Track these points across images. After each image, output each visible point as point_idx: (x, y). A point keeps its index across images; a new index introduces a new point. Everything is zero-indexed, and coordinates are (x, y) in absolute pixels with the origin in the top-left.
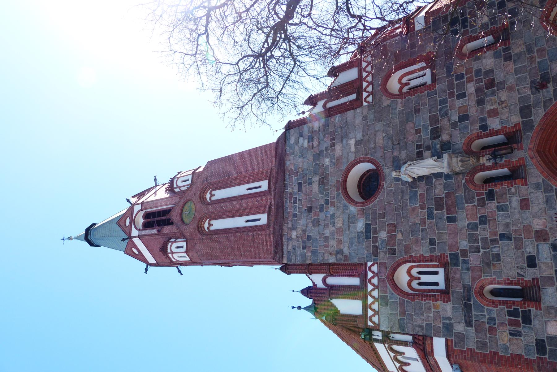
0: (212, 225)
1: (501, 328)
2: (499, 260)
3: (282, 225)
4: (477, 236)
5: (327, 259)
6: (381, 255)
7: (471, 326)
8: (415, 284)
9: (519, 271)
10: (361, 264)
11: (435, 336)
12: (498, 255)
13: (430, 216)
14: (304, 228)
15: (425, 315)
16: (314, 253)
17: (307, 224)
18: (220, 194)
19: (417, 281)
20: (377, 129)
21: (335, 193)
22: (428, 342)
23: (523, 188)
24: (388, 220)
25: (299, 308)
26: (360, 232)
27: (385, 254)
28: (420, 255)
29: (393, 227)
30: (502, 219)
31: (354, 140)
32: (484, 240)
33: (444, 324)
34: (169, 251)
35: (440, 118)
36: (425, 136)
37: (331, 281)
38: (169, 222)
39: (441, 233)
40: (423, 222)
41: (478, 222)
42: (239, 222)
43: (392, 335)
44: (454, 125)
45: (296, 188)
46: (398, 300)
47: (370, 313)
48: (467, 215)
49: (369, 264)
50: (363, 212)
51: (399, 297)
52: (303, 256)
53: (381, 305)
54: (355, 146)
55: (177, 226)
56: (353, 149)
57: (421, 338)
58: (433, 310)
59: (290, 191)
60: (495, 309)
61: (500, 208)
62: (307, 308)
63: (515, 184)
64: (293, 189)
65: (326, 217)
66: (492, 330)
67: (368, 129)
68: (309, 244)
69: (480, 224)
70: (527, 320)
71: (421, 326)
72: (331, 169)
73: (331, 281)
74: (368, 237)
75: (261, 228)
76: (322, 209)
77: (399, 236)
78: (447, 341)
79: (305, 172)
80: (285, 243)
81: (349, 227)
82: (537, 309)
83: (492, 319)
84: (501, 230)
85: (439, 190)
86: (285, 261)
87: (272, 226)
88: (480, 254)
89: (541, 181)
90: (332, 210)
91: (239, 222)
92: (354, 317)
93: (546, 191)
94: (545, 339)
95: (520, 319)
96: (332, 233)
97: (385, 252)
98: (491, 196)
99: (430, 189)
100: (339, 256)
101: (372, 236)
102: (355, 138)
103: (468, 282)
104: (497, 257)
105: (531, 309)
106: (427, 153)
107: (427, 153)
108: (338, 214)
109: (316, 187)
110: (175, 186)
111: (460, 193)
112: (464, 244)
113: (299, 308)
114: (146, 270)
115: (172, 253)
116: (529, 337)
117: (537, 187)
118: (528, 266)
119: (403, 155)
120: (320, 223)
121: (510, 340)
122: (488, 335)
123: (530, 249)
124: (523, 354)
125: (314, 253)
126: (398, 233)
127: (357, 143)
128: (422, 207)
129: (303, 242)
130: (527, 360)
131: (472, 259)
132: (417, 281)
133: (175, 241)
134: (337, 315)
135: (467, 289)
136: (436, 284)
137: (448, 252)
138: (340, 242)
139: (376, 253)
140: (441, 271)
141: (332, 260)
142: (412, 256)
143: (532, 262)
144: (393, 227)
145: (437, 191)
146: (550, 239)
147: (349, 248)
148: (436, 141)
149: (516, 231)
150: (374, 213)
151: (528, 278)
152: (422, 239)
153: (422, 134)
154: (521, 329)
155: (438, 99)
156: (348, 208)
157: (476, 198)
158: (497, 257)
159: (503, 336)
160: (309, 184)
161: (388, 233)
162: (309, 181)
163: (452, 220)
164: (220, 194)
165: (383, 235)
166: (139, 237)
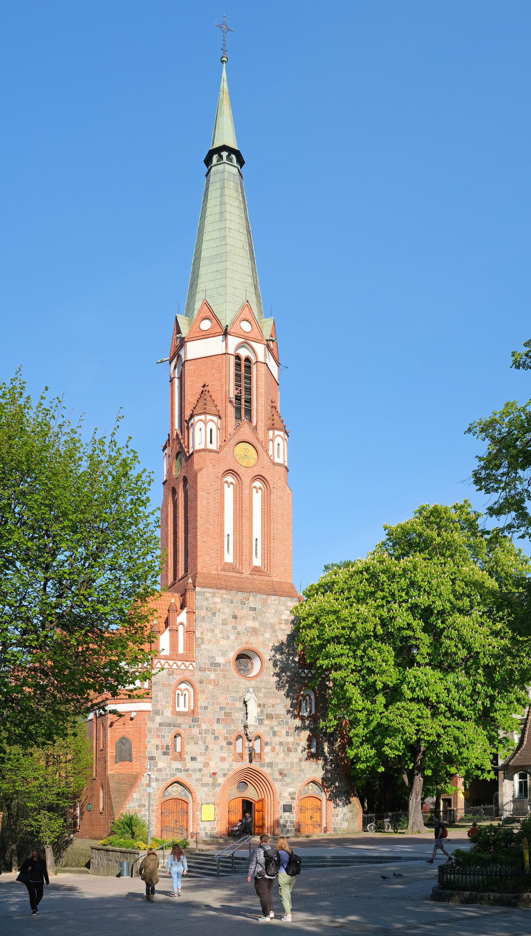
2: (195, 744)
3: (226, 589)
6: (200, 673)
13: (222, 708)
14: (221, 610)
16: (203, 619)
17: (224, 614)
19: (180, 694)
21: (244, 641)
23: (230, 759)
24: (221, 680)
29: (216, 684)
30: (216, 747)
32: (206, 738)
36: (270, 710)
40: (218, 704)
44: (272, 728)
49: (194, 664)
52: (201, 608)
55: (234, 435)
61: (222, 747)
68: (209, 614)
72: (261, 639)
74: (211, 664)
76: (234, 628)
77: (211, 687)
79: (263, 614)
90: (232, 637)
93: (228, 769)
98: (229, 743)
99: (238, 710)
100: (200, 640)
106: (259, 710)
111: (233, 727)
112: (204, 727)
117: (231, 766)
123: (199, 759)
125: (203, 619)
128: (227, 704)
129: (211, 609)
132: (180, 694)
135: (179, 726)
138: (210, 641)
139: (201, 670)
140: (186, 710)
141: (198, 634)
143: (193, 759)
144: (216, 684)
145: (236, 714)
148: (265, 717)
150: (227, 671)
151: (185, 756)
158: (196, 743)
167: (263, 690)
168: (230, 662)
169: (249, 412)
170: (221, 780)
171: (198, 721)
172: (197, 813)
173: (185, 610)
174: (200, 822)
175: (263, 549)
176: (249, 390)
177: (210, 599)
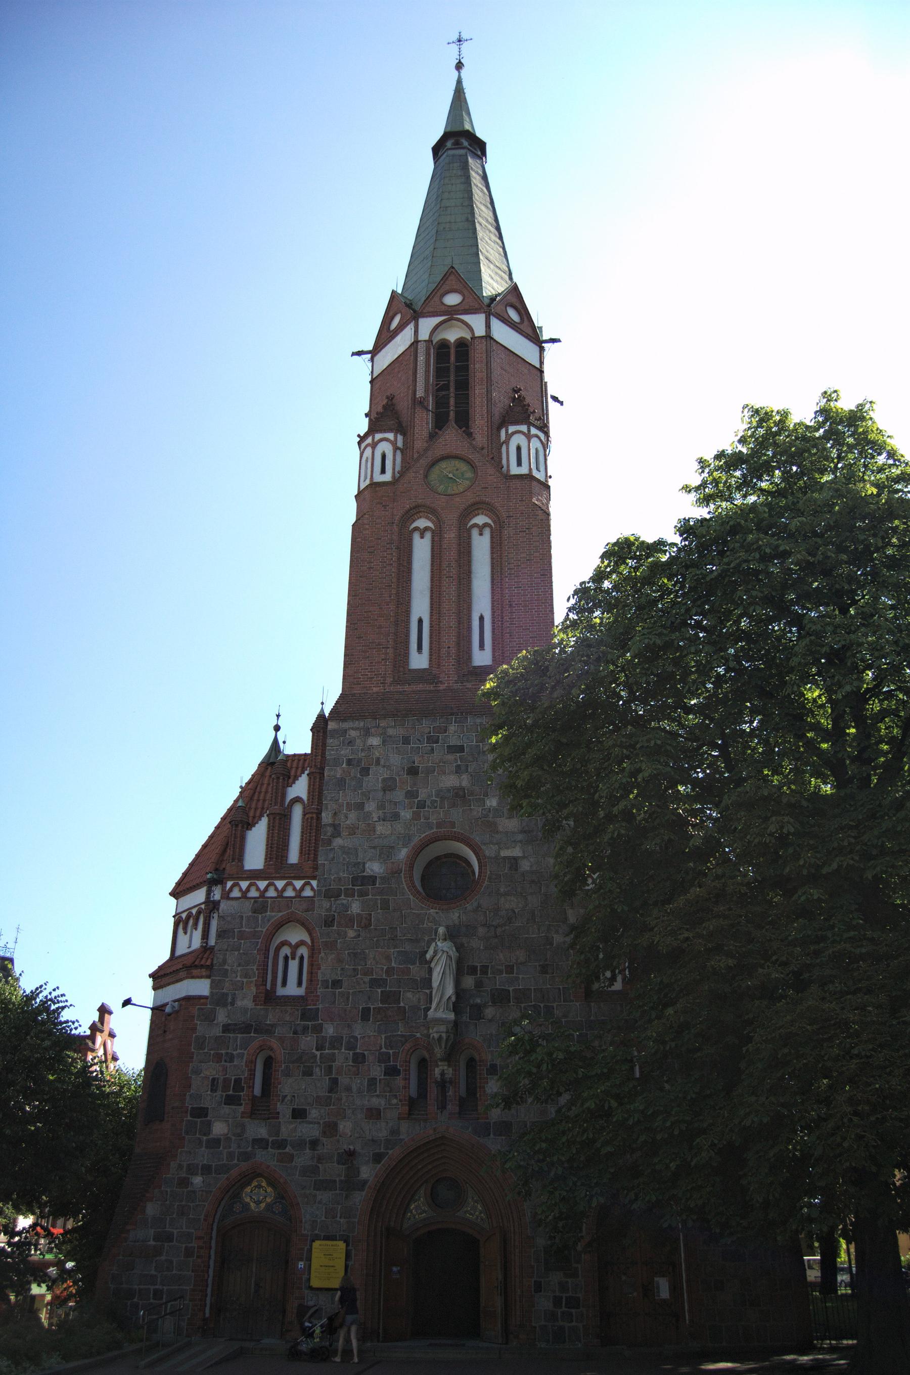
0: (422, 537)
1: (221, 1069)
4: (337, 1049)
5: (327, 808)
6: (326, 904)
7: (224, 1032)
8: (286, 950)
9: (289, 1098)
10: (316, 868)
11: (212, 983)
12: (310, 1074)
13: (375, 983)
14: (382, 762)
15: (239, 968)
16: (341, 783)
17: (388, 767)
18: (481, 546)
19: (289, 955)
20: (529, 898)
21: (433, 820)
22: (204, 972)
25: (277, 728)
26: (364, 866)
27: (327, 910)
28: (319, 965)
31: (520, 855)
32: (332, 1058)
33: (227, 994)
34: (378, 436)
35: (523, 1005)
37: (297, 813)
38: (440, 422)
39: (348, 999)
41: (358, 1051)
42: (420, 606)
43: (216, 915)
45: (454, 742)
46: (260, 929)
47: (244, 884)
48: (369, 1037)
49: (314, 883)
50: (396, 873)
51: (264, 930)
52: (337, 762)
53: (255, 902)
54: (509, 858)
56: (505, 853)
57: (208, 963)
58: (245, 980)
59: (452, 728)
60: (243, 1064)
61: (372, 1082)
62: (276, 742)
63: (402, 1105)
64: (454, 734)
65: (395, 803)
66: (218, 1058)
67: (533, 881)
68: (355, 772)
69: (354, 1054)
70: (231, 1100)
71: (224, 962)
73: (297, 813)
74: (354, 880)
75: (405, 655)
76: (411, 795)
77: (351, 933)
78: (206, 998)
80: (362, 724)
81: (374, 848)
82: (243, 1113)
83: (231, 1058)
84: (344, 1080)
85: (409, 998)
86: (331, 726)
87: (399, 688)
88: (314, 1051)
89: (401, 1137)
91: (420, 606)
92: (239, 856)
94: (209, 1118)
95: (231, 1092)
96: (368, 815)
97: (329, 910)
98: (392, 1072)
100: (330, 830)
101: (356, 888)
102: (524, 857)
103: (278, 1031)
104: (308, 1073)
105: (242, 1107)
106: (469, 982)
107: (469, 982)
108: (399, 828)
109: (450, 781)
110: (512, 429)
111: (401, 1030)
112: (330, 1030)
113: (277, 728)
114: (359, 353)
115: (374, 445)
116: (209, 1100)
117: (395, 1132)
118: (294, 1110)
119: (475, 943)
120: (387, 792)
121: (207, 1077)
122: (212, 1052)
123: (314, 1113)
124: (192, 1091)
125: (341, 783)
126: (356, 930)
127: (514, 862)
128: (389, 971)
129: (359, 761)
130: (185, 1095)
131: (308, 1039)
133: (396, 449)
134: (243, 827)
135: (269, 1030)
136: (284, 983)
137: (320, 1006)
140: (301, 992)
141: (326, 818)
142: (320, 953)
143: (299, 1114)
145: (409, 995)
146: (325, 1139)
147: (342, 847)
149: (340, 1099)
152: (342, 969)
153: (504, 975)
154: (219, 1093)
155: (555, 1005)
156: (404, 846)
157: (391, 1052)
158: (308, 1073)
159: (211, 1070)
160: (458, 767)
161: (358, 915)
162: (463, 768)
163: (365, 1014)
164: (481, 546)
165: (356, 908)
166: (416, 342)
167: (481, 931)
168: (399, 872)
169: (464, 421)
170: (367, 1172)
171: (315, 1018)
172: (301, 1265)
173: (306, 772)
174: (306, 1291)
175: (494, 640)
176: (463, 386)
177: (358, 741)
